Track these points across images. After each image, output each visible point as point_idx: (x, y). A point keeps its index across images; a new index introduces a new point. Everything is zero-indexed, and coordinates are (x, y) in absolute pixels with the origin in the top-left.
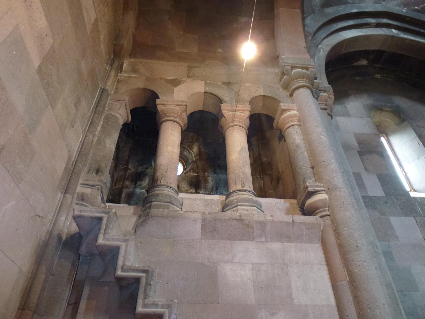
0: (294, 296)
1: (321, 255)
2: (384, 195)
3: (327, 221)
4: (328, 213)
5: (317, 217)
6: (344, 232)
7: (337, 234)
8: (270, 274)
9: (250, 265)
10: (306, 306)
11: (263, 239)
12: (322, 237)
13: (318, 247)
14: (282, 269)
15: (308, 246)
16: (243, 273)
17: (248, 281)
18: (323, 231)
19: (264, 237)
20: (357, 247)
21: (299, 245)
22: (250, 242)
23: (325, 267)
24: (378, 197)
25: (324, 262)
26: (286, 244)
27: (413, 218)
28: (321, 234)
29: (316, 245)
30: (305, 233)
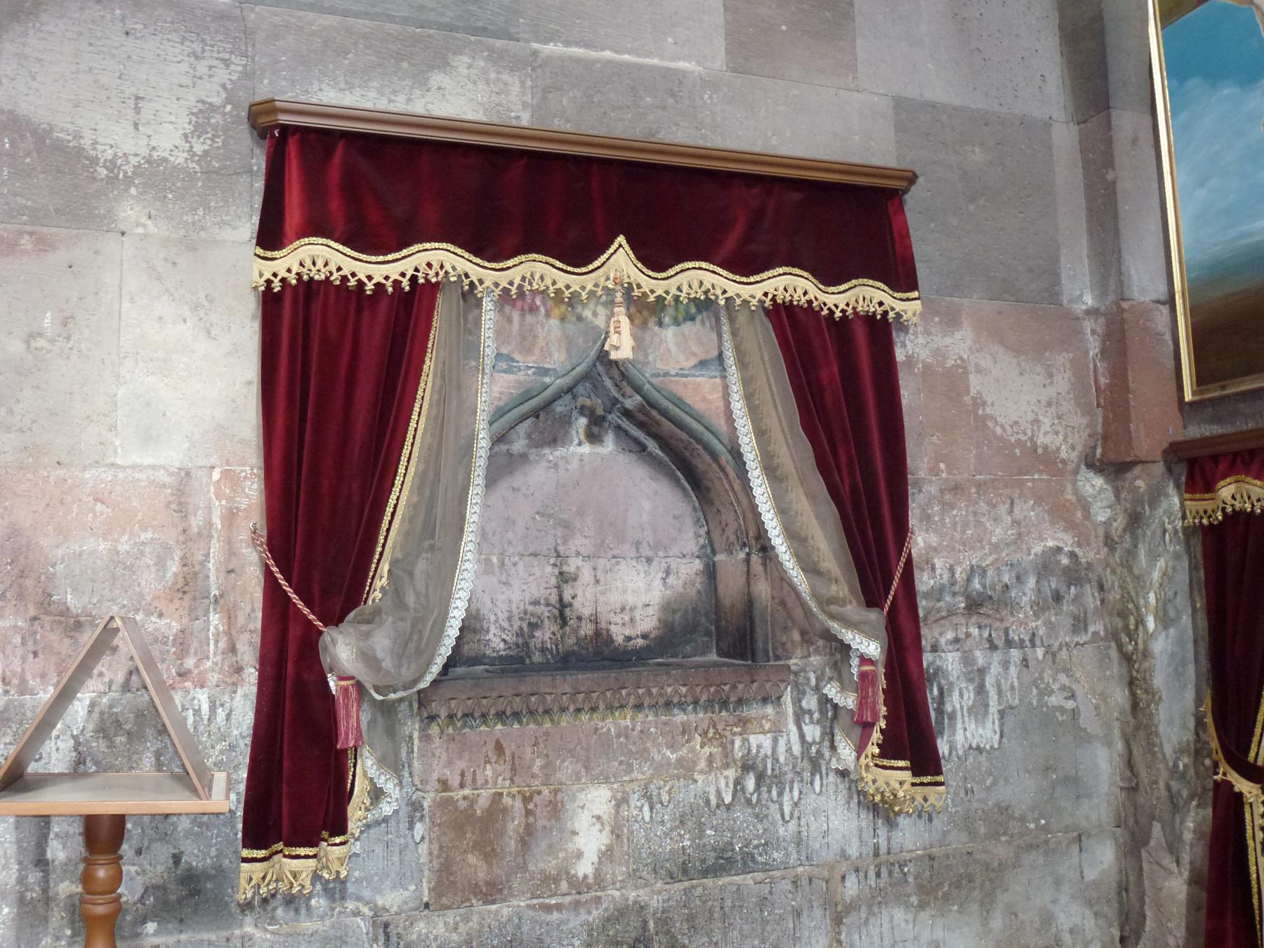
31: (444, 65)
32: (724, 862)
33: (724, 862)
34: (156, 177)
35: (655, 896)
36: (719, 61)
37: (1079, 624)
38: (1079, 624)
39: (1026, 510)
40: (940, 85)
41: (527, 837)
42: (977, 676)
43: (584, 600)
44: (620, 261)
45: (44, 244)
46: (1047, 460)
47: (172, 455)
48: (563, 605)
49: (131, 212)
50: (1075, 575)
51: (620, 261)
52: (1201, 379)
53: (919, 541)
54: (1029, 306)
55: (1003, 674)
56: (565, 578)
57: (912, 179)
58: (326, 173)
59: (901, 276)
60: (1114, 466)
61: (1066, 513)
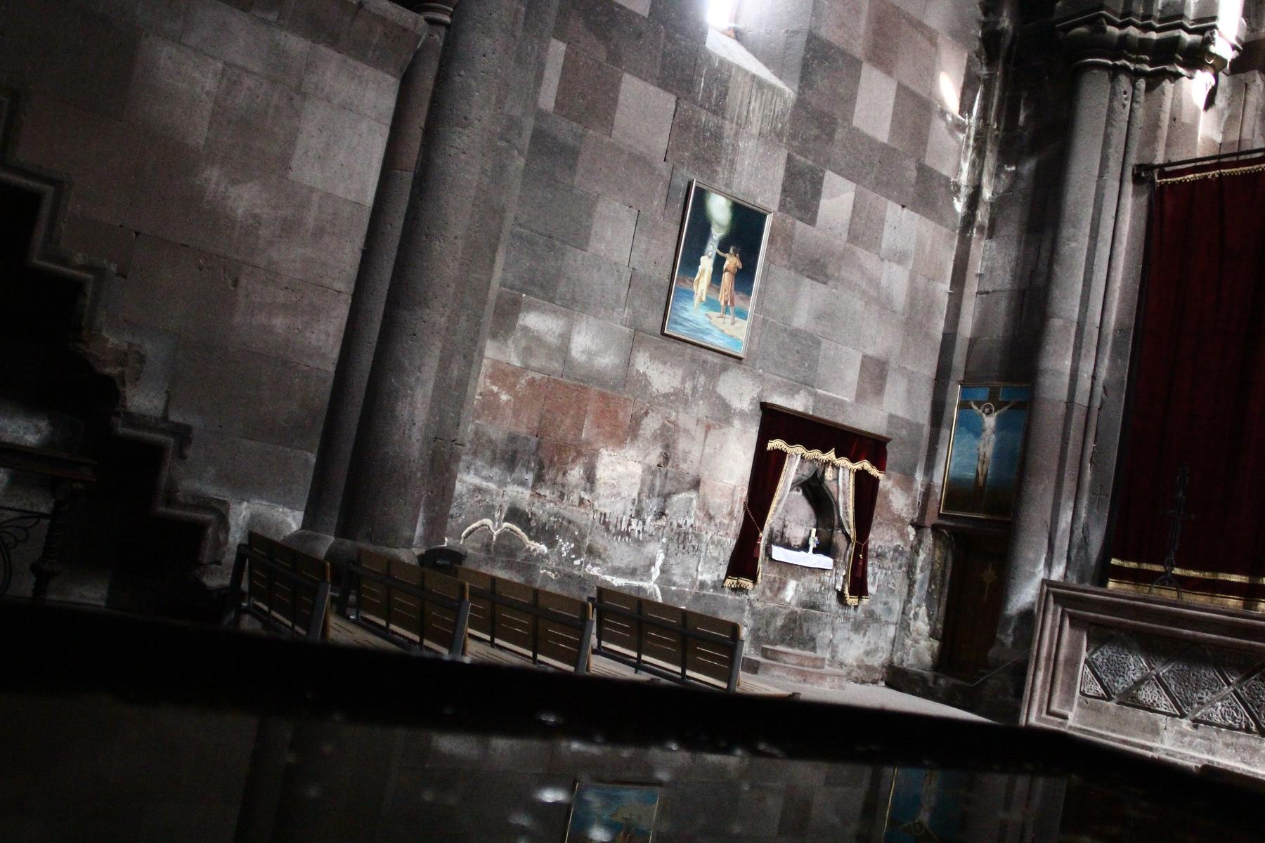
0: (293, 164)
1: (388, 103)
2: (646, 14)
3: (437, 36)
4: (447, 19)
5: (421, 18)
6: (457, 79)
7: (443, 77)
8: (258, 101)
9: (220, 65)
10: (312, 190)
11: (272, 17)
12: (412, 65)
13: (391, 83)
14: (291, 99)
15: (369, 72)
16: (197, 75)
17: (204, 96)
18: (417, 54)
19: (276, 13)
20: (466, 118)
21: (351, 61)
22: (237, 12)
23: (386, 131)
24: (631, 12)
25: (389, 121)
26: (322, 49)
27: (673, 98)
28: (411, 57)
29: (388, 76)
30: (375, 42)
31: (798, 392)
32: (814, 606)
33: (814, 606)
34: (742, 414)
35: (799, 610)
36: (853, 399)
37: (900, 567)
38: (900, 567)
39: (895, 533)
40: (900, 413)
41: (779, 589)
42: (875, 574)
43: (788, 533)
44: (831, 455)
45: (720, 427)
46: (902, 520)
47: (733, 482)
48: (783, 533)
49: (737, 423)
50: (902, 553)
51: (831, 455)
52: (946, 508)
53: (871, 536)
54: (906, 481)
55: (880, 575)
56: (785, 526)
57: (889, 440)
58: (775, 422)
59: (881, 468)
60: (918, 526)
61: (903, 535)
